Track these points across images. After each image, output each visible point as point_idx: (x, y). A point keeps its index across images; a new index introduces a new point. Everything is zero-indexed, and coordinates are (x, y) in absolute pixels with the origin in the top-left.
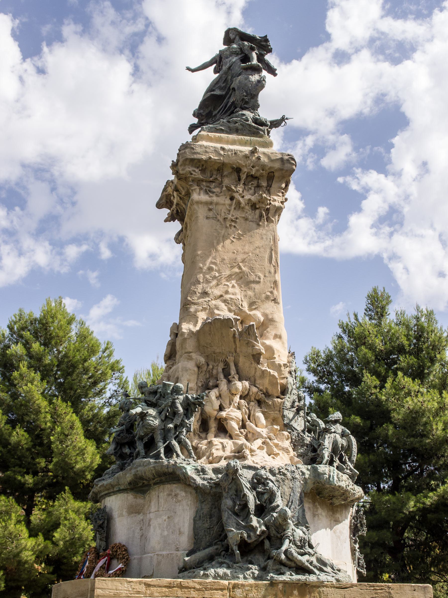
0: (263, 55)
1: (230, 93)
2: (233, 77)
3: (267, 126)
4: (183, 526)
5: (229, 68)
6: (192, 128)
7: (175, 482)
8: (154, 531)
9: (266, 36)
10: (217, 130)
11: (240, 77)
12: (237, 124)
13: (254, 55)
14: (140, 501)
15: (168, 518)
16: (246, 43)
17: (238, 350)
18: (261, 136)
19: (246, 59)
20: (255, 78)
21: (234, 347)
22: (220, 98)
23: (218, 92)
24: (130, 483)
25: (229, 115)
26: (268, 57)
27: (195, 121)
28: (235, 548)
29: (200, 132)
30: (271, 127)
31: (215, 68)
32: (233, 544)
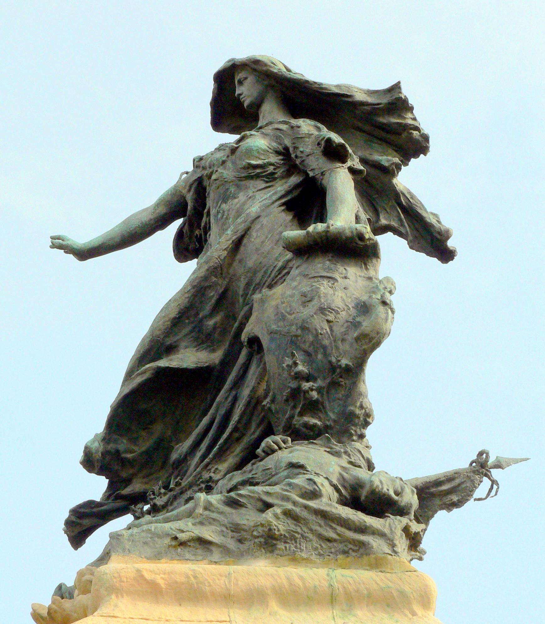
0: (389, 172)
1: (242, 359)
2: (253, 286)
3: (402, 512)
5: (238, 244)
6: (82, 523)
9: (396, 87)
10: (183, 544)
11: (279, 290)
12: (269, 515)
13: (342, 187)
16: (306, 126)
18: (378, 564)
19: (308, 201)
20: (344, 285)
22: (200, 382)
23: (188, 358)
25: (239, 466)
26: (411, 179)
27: (96, 487)
29: (104, 558)
30: (423, 516)
31: (180, 235)
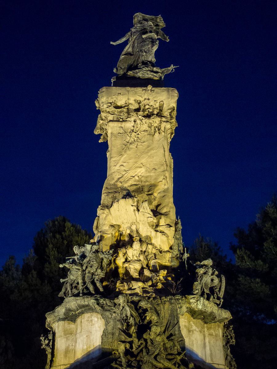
4: (96, 342)
7: (91, 311)
8: (79, 346)
14: (72, 326)
15: (87, 336)
21: (135, 218)
24: (65, 314)
28: (122, 355)
32: (121, 352)
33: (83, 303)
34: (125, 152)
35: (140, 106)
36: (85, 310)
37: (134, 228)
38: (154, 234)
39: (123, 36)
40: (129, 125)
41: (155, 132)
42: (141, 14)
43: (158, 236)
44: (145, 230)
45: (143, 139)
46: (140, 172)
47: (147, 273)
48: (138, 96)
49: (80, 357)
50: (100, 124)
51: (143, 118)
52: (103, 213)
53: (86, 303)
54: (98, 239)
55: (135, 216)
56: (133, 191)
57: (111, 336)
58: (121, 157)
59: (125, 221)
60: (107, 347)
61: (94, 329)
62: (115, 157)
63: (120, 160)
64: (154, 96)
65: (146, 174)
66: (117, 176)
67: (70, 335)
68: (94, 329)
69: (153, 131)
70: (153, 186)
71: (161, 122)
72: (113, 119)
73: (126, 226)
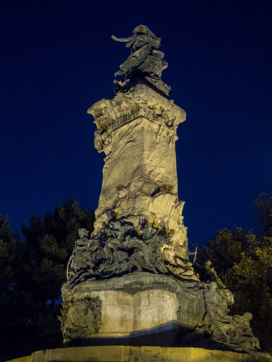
4: (169, 316)
15: (158, 310)
17: (172, 214)
21: (170, 212)
33: (161, 280)
34: (154, 150)
35: (162, 113)
36: (157, 286)
37: (166, 220)
38: (178, 230)
39: (126, 37)
40: (155, 127)
41: (170, 142)
42: (147, 28)
43: (180, 232)
44: (173, 224)
45: (163, 143)
46: (162, 171)
47: (179, 262)
48: (164, 105)
49: (149, 328)
50: (99, 106)
51: (165, 126)
52: (146, 200)
53: (165, 281)
54: (143, 222)
55: (171, 210)
56: (161, 187)
57: (187, 314)
58: (151, 153)
59: (161, 212)
60: (185, 323)
61: (166, 305)
62: (147, 151)
63: (151, 155)
64: (174, 111)
65: (166, 175)
66: (149, 170)
67: (127, 305)
68: (166, 305)
69: (168, 139)
70: (171, 187)
71: (174, 135)
72: (145, 116)
73: (159, 217)
